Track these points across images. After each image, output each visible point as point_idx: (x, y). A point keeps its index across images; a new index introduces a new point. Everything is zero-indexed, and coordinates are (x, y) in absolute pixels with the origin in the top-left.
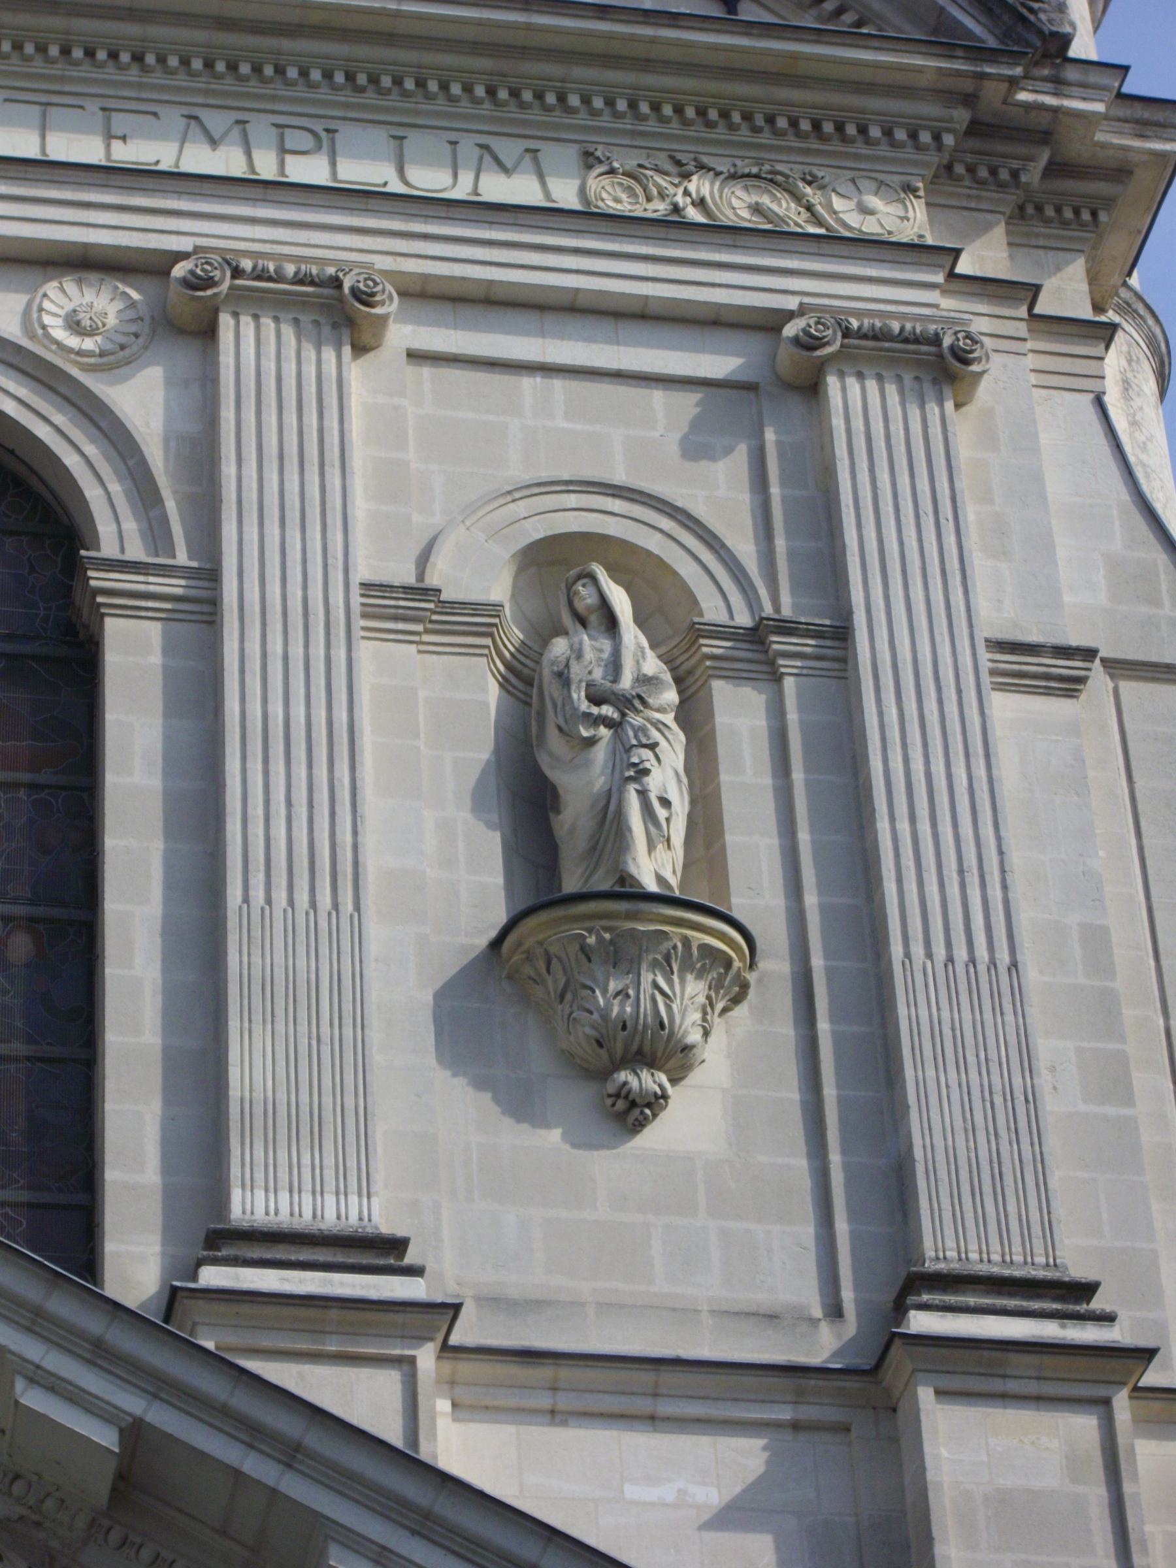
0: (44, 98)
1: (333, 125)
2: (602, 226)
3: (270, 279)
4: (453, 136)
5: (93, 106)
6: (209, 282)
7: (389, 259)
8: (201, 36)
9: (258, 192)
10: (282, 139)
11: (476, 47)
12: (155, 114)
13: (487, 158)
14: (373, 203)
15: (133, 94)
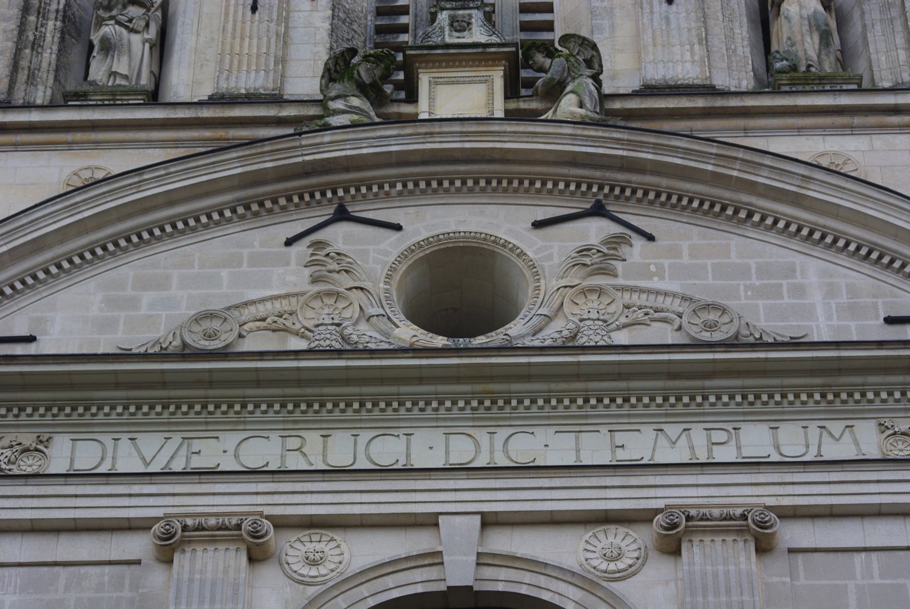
0: (577, 428)
1: (737, 425)
2: (891, 466)
3: (707, 520)
4: (805, 423)
5: (604, 430)
6: (674, 526)
7: (774, 499)
8: (659, 384)
9: (698, 470)
10: (709, 437)
11: (812, 373)
12: (639, 430)
13: (825, 434)
14: (763, 468)
15: (626, 421)
